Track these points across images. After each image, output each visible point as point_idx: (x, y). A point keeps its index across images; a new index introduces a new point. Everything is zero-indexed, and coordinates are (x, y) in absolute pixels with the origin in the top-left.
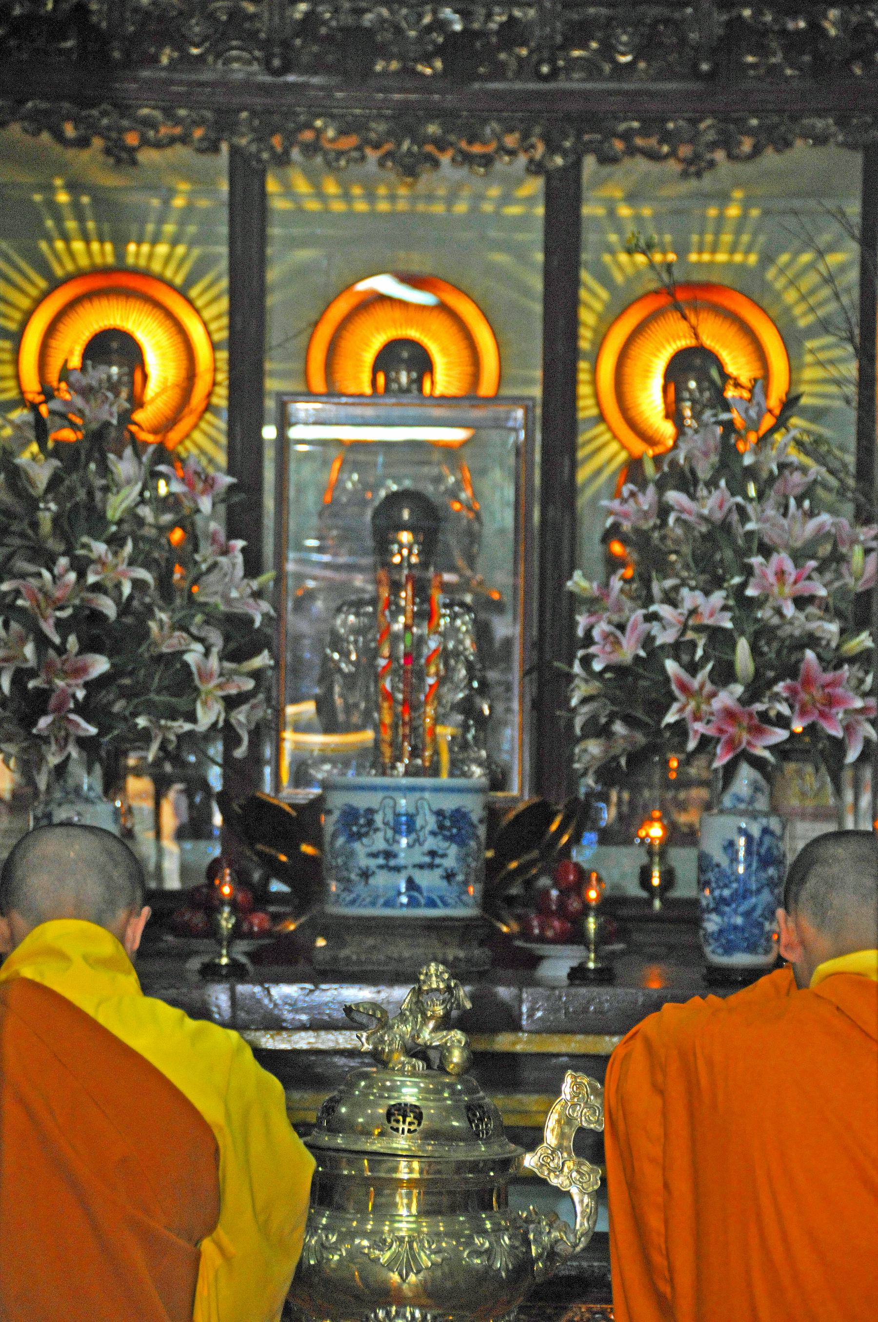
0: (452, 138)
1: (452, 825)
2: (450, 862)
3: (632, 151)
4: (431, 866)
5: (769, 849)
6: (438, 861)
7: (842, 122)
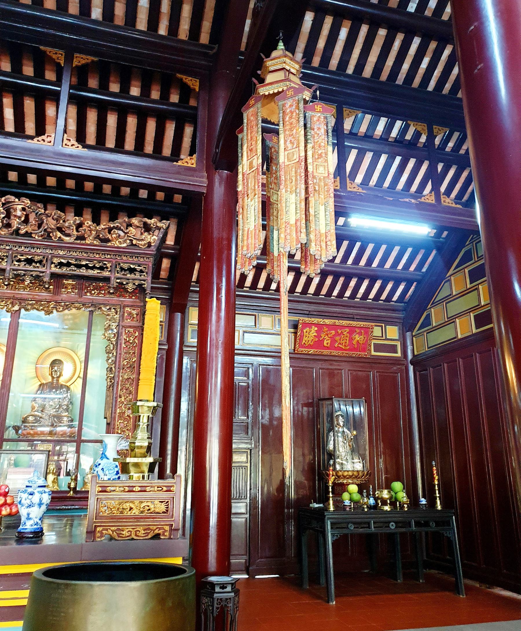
7: (83, 305)
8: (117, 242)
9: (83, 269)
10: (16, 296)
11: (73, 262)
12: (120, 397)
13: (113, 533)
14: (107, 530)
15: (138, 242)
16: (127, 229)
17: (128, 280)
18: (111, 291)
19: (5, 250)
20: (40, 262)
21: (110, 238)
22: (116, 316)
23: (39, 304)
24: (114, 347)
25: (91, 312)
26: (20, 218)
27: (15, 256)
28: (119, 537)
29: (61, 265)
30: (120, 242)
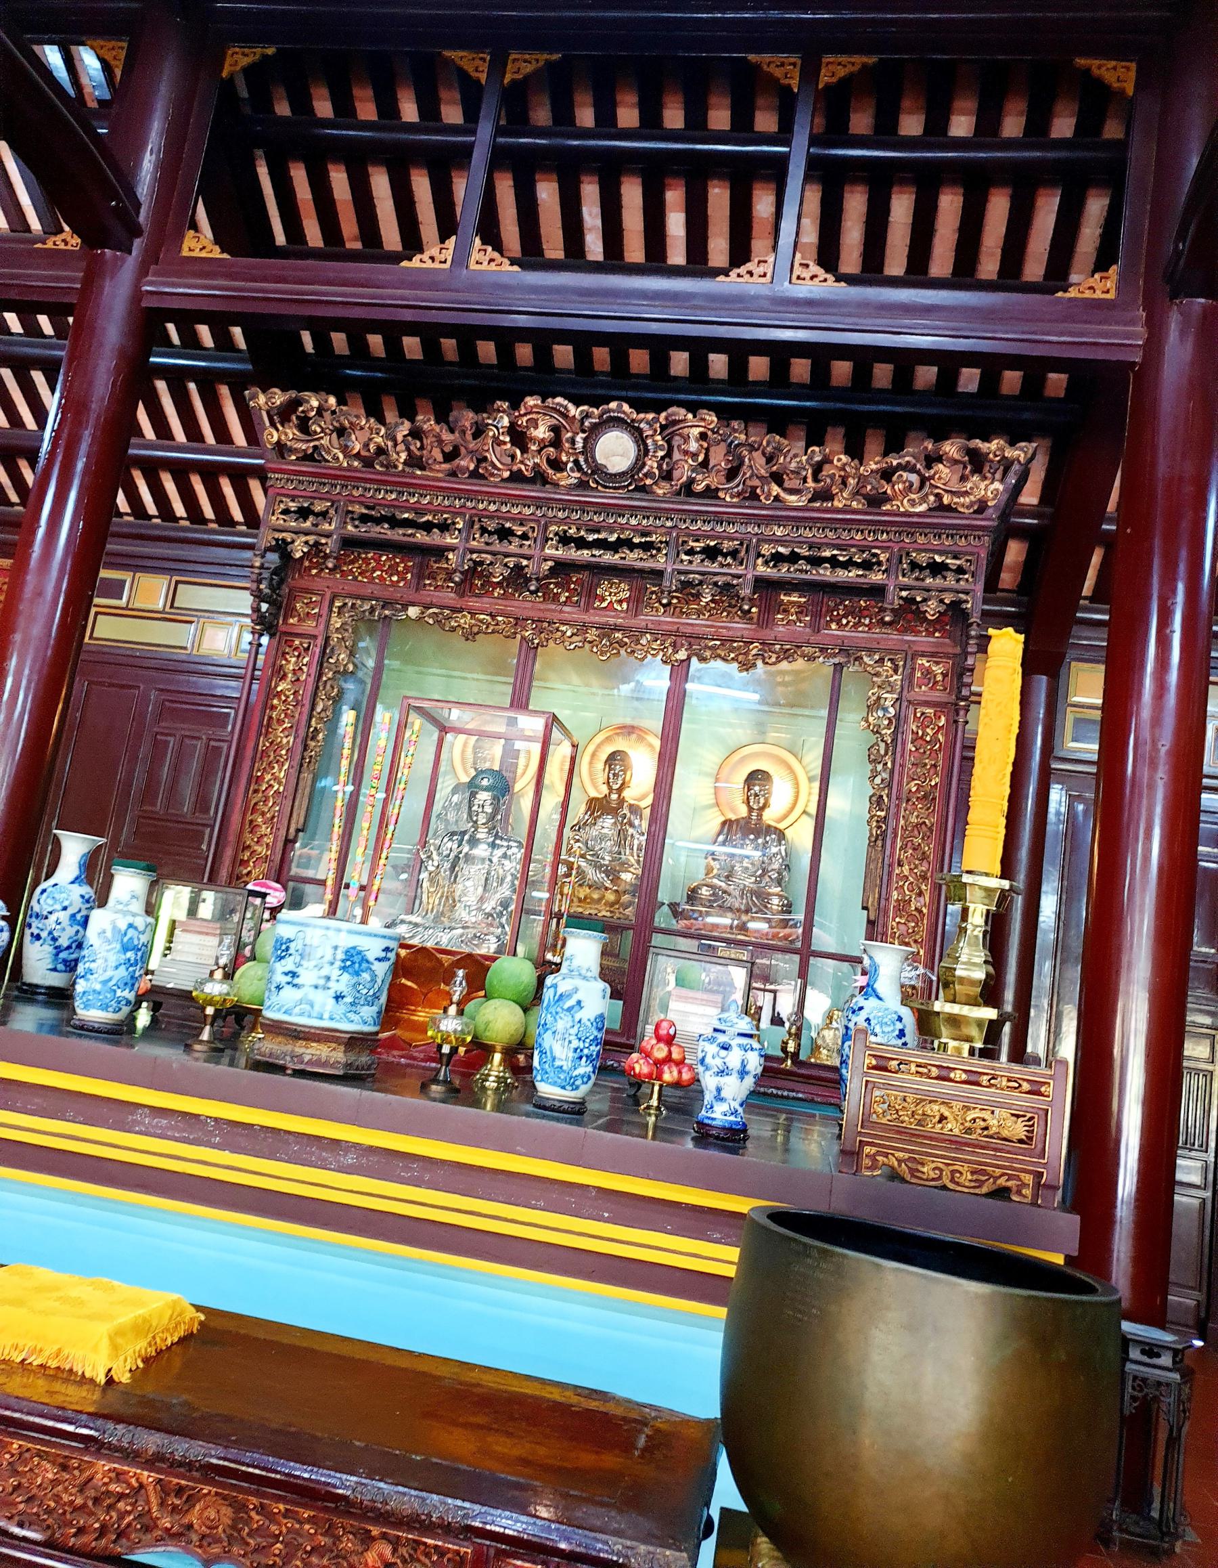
1: (353, 961)
7: (822, 650)
8: (905, 501)
9: (826, 568)
10: (682, 629)
11: (804, 551)
12: (900, 865)
13: (900, 1165)
14: (886, 1155)
15: (956, 500)
16: (929, 467)
17: (928, 591)
18: (887, 619)
19: (664, 530)
20: (734, 553)
21: (889, 492)
22: (895, 677)
23: (727, 648)
24: (886, 752)
25: (839, 668)
26: (694, 456)
27: (684, 542)
28: (913, 1176)
29: (777, 558)
30: (914, 500)
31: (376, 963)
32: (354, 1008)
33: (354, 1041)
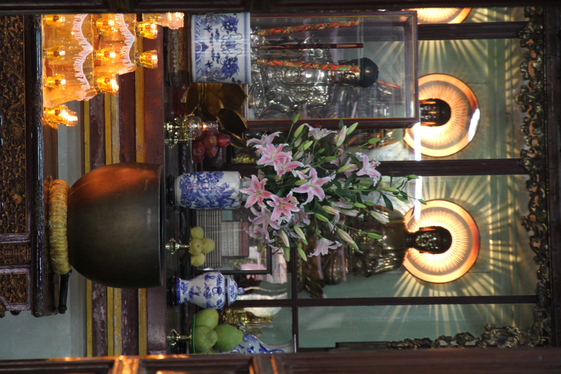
0: (535, 117)
1: (231, 65)
2: (215, 65)
3: (533, 195)
4: (213, 57)
5: (226, 202)
6: (215, 59)
7: (548, 284)
31: (231, 79)
32: (204, 73)
33: (186, 74)
